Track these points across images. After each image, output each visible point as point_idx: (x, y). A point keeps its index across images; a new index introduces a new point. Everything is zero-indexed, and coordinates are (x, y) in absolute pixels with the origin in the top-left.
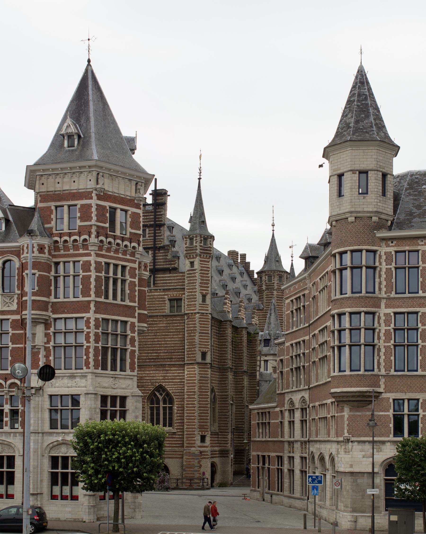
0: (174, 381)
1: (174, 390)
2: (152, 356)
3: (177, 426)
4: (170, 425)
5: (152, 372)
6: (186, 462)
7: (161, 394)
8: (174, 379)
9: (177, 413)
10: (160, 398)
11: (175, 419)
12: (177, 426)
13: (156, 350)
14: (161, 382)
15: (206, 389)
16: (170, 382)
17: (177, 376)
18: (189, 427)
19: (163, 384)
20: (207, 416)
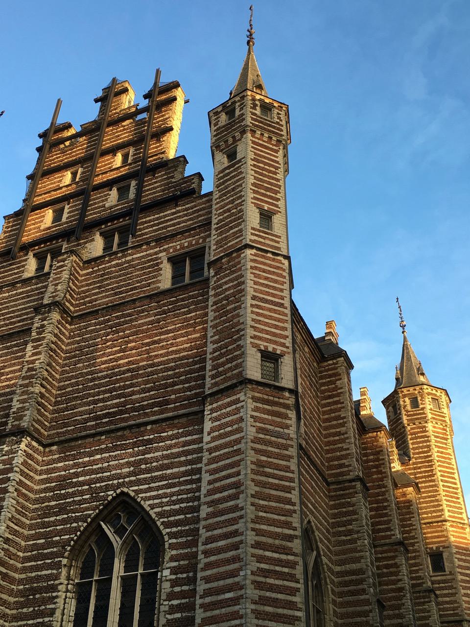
0: (169, 471)
1: (168, 504)
2: (106, 407)
5: (98, 457)
8: (168, 467)
9: (171, 596)
10: (116, 541)
13: (120, 388)
15: (281, 478)
17: (179, 455)
19: (131, 491)
20: (293, 592)
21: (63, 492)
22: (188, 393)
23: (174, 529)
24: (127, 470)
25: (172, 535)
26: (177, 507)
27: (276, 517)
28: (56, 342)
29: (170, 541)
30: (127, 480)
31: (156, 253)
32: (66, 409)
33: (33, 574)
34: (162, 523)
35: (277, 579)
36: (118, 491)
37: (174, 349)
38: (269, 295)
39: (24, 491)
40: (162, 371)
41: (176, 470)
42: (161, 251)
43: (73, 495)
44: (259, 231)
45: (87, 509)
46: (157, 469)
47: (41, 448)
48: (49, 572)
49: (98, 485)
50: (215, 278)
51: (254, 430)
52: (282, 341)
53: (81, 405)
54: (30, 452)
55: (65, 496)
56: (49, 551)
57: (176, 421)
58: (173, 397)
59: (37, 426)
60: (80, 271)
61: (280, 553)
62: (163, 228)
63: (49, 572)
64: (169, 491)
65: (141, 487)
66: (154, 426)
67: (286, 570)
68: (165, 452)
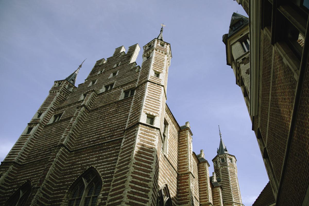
1: (106, 170)
2: (93, 138)
15: (148, 159)
21: (72, 167)
22: (121, 132)
23: (107, 180)
24: (95, 159)
25: (105, 182)
26: (109, 171)
27: (143, 173)
28: (81, 118)
29: (104, 184)
30: (94, 162)
31: (120, 90)
32: (80, 140)
33: (56, 196)
34: (103, 177)
35: (139, 196)
36: (90, 166)
37: (120, 118)
38: (154, 97)
39: (59, 166)
40: (114, 125)
41: (111, 158)
42: (122, 89)
43: (76, 168)
44: (154, 77)
45: (79, 173)
46: (105, 158)
47: (69, 152)
48: (61, 195)
49: (84, 164)
50: (136, 93)
51: (139, 140)
52: (157, 112)
53: (85, 138)
54: (64, 152)
55: (73, 169)
56: (63, 187)
57: (115, 142)
58: (116, 133)
59: (68, 144)
60: (95, 97)
61: (142, 186)
62: (124, 82)
63: (61, 195)
64: (107, 166)
65: (98, 165)
66: (107, 144)
67: (144, 193)
68: (109, 153)
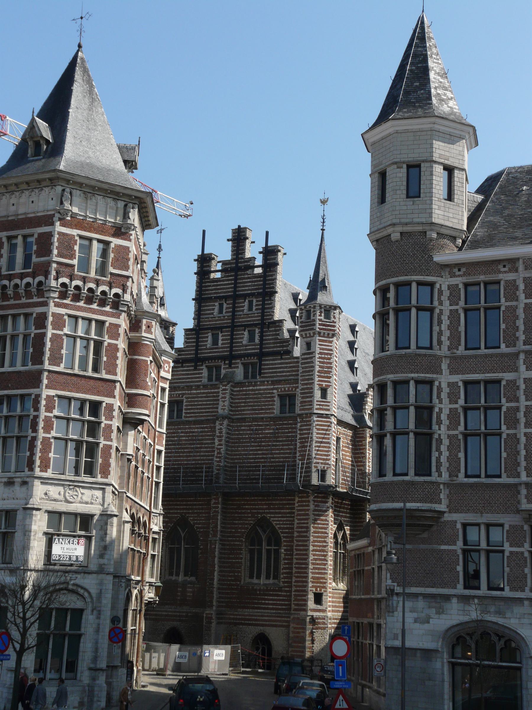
0: (282, 511)
1: (282, 524)
3: (285, 578)
4: (276, 577)
6: (293, 632)
7: (265, 532)
11: (282, 567)
12: (285, 578)
14: (264, 513)
16: (276, 513)
18: (298, 579)
25: (284, 537)
26: (286, 526)
41: (285, 511)
